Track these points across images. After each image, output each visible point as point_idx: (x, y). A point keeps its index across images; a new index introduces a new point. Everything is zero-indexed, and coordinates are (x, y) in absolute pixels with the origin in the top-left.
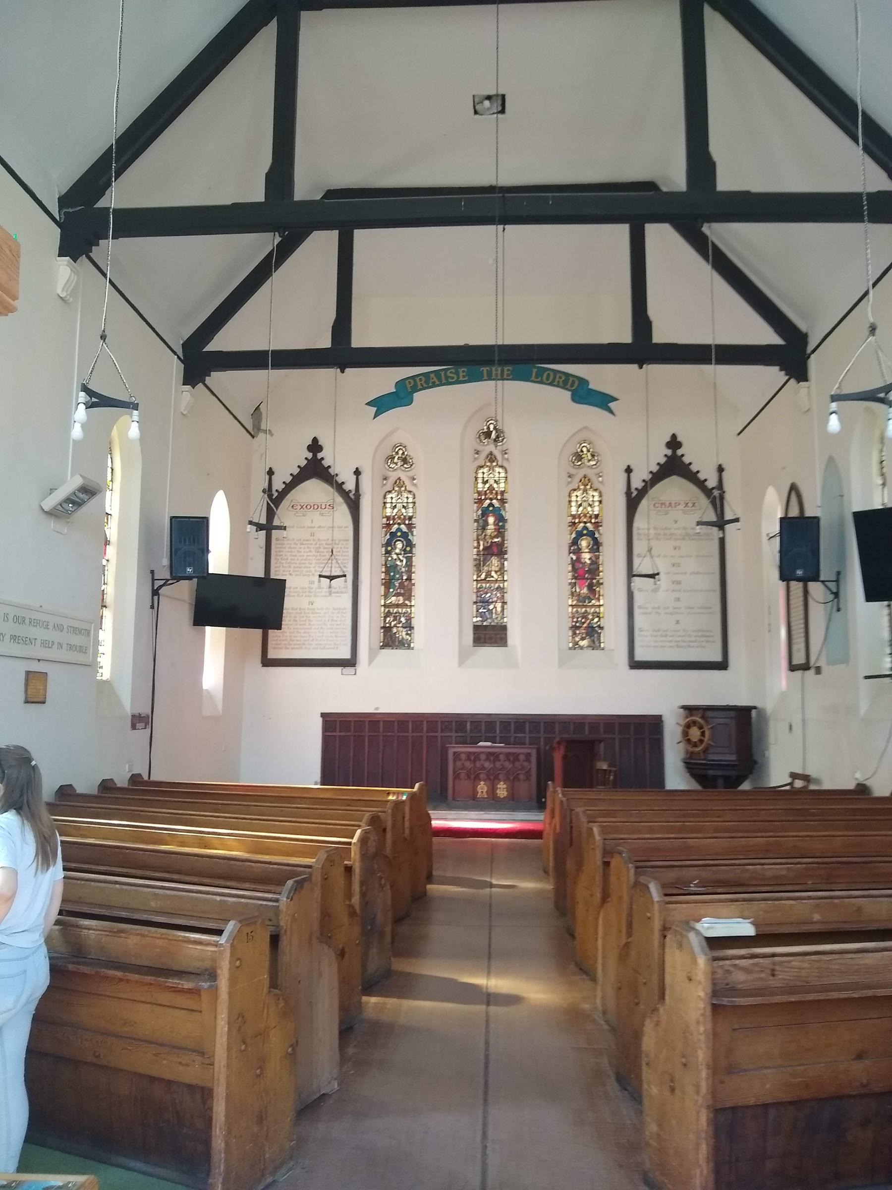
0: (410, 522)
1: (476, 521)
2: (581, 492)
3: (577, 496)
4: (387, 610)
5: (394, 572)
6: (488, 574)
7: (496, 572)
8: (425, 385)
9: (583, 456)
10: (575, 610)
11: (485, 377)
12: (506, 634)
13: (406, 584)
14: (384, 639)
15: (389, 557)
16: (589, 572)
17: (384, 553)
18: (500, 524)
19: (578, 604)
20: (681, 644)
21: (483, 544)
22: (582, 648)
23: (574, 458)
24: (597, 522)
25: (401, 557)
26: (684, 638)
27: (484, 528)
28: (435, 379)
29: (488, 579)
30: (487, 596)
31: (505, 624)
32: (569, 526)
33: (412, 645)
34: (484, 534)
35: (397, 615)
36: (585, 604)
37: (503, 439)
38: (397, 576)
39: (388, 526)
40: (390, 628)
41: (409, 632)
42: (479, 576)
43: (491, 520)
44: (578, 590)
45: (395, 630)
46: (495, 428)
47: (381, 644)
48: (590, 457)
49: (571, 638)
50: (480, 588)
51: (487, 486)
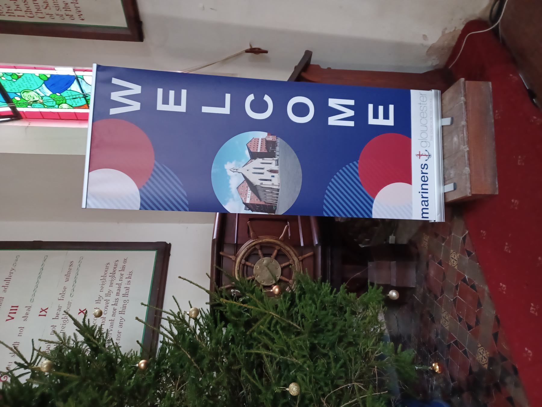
20: (119, 308)
26: (112, 302)
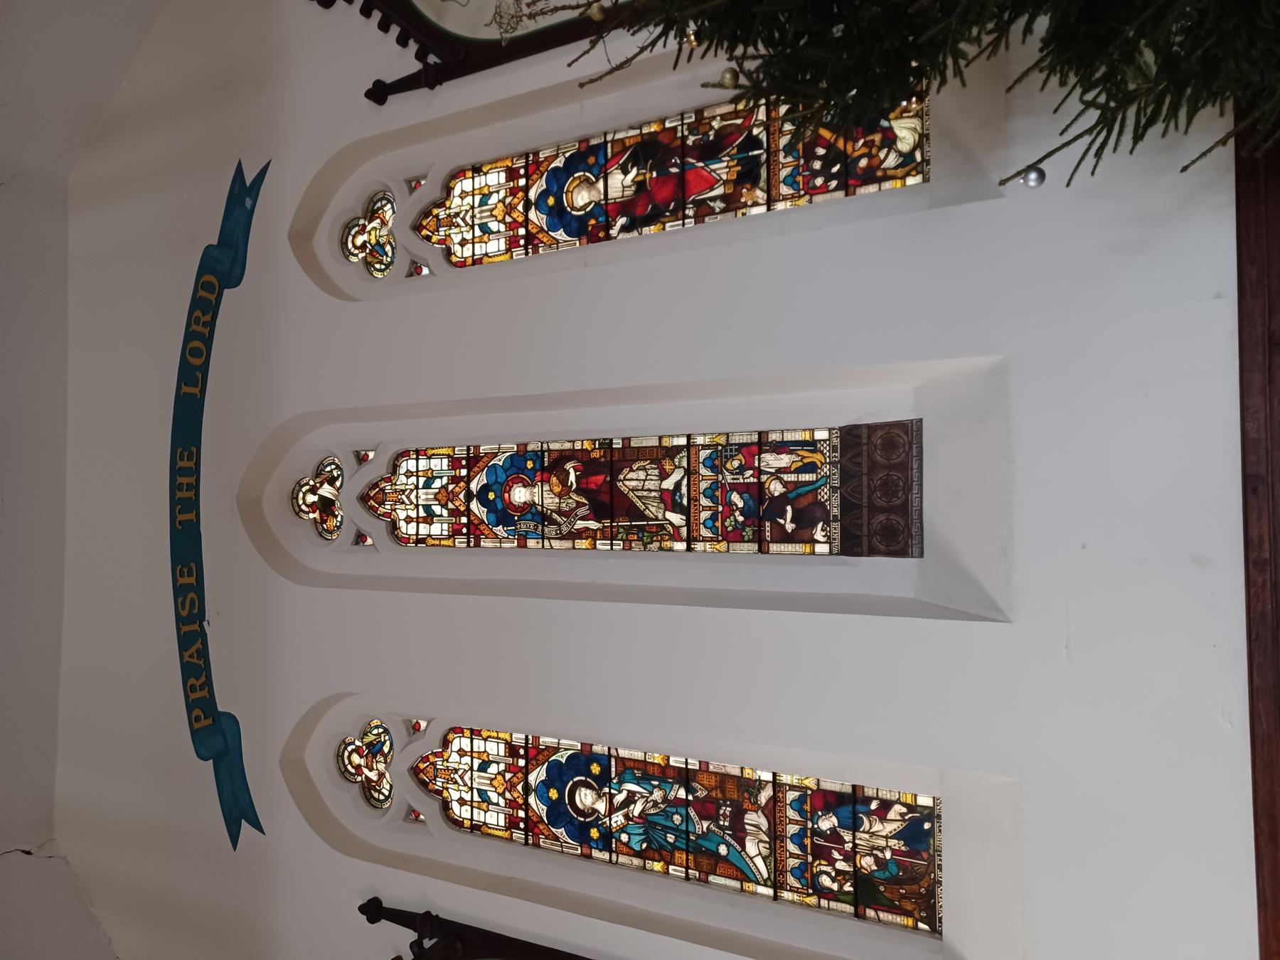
0: (522, 752)
1: (522, 545)
2: (454, 230)
3: (463, 243)
4: (791, 880)
5: (666, 829)
6: (670, 500)
7: (664, 476)
8: (203, 679)
9: (373, 241)
10: (785, 190)
11: (191, 516)
12: (872, 428)
13: (701, 794)
14: (907, 914)
15: (618, 840)
16: (661, 166)
17: (606, 856)
18: (530, 465)
19: (762, 184)
21: (583, 518)
22: (923, 140)
23: (378, 266)
24: (526, 167)
25: (620, 798)
27: (543, 518)
28: (193, 650)
29: (685, 502)
30: (741, 505)
31: (836, 434)
32: (536, 251)
33: (924, 801)
34: (555, 516)
35: (808, 842)
36: (765, 156)
37: (338, 467)
38: (677, 819)
39: (531, 825)
40: (858, 877)
41: (874, 806)
42: (676, 537)
43: (520, 495)
44: (719, 191)
45: (867, 863)
46: (313, 490)
47: (921, 925)
48: (376, 223)
49: (887, 185)
50: (713, 529)
51: (437, 509)
